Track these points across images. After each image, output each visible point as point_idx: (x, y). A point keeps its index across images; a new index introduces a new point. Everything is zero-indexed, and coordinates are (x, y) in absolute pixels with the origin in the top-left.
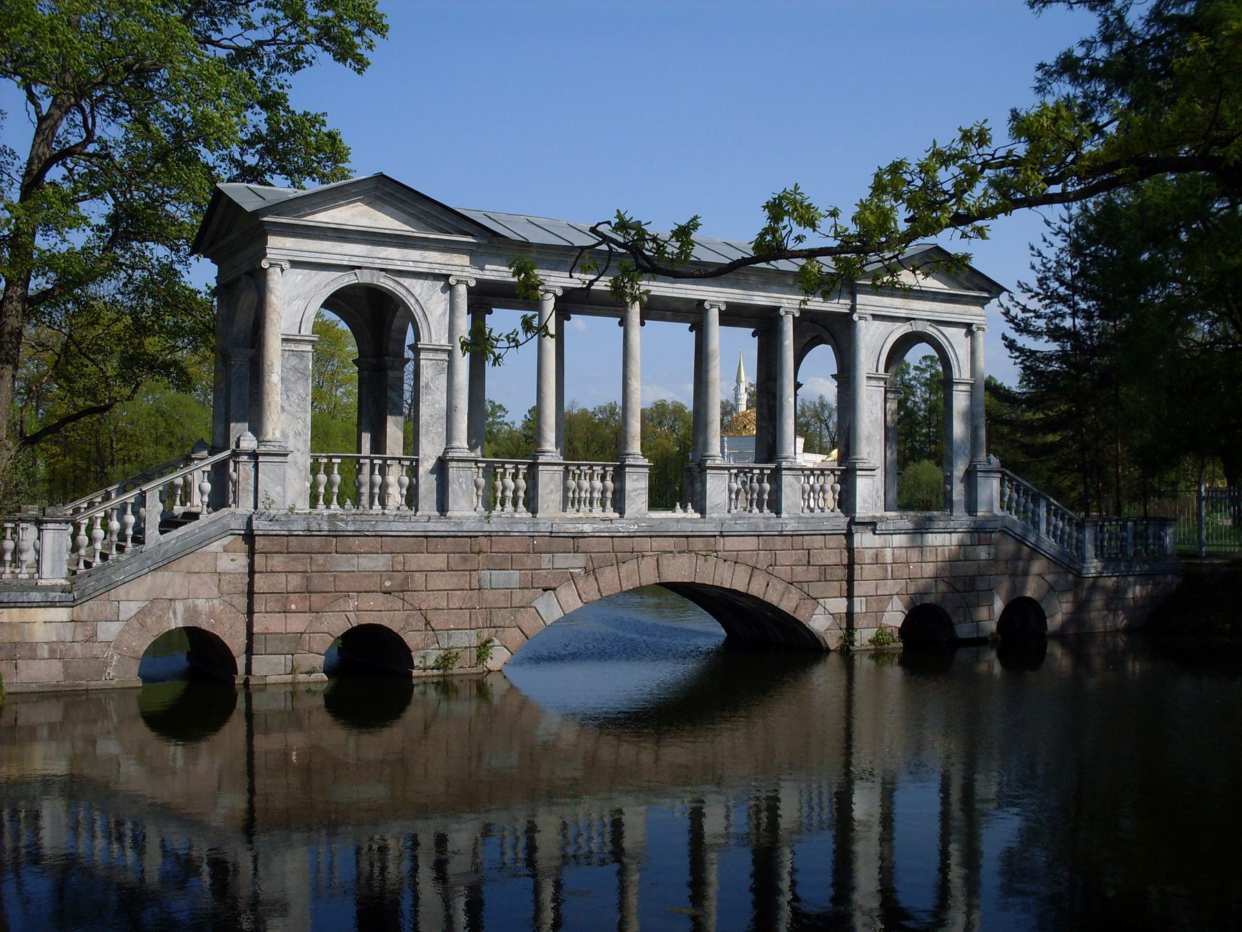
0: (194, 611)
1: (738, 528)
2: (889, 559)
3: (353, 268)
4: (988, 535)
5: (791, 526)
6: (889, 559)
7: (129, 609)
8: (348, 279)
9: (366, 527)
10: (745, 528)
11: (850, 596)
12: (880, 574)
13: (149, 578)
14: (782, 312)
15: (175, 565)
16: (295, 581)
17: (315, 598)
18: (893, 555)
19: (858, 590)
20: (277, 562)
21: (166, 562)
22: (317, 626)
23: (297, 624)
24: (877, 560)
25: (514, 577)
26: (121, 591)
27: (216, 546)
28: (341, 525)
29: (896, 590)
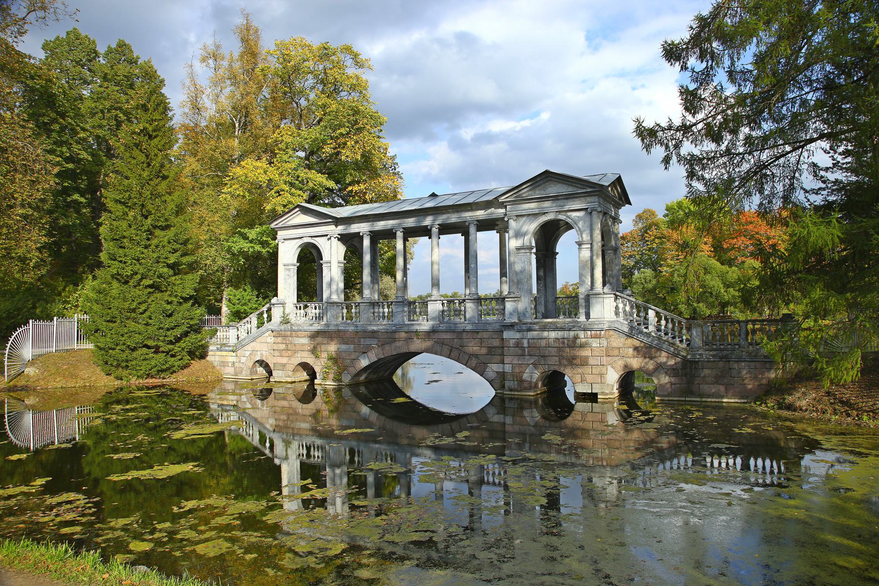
0: (262, 355)
1: (441, 328)
2: (526, 345)
3: (301, 238)
4: (598, 332)
5: (469, 327)
6: (526, 345)
7: (248, 353)
8: (300, 242)
9: (300, 328)
10: (444, 328)
11: (503, 363)
12: (520, 352)
13: (252, 344)
14: (467, 224)
15: (257, 340)
16: (283, 346)
17: (289, 352)
18: (528, 343)
19: (507, 360)
20: (279, 340)
21: (254, 340)
22: (290, 362)
23: (284, 360)
24: (518, 344)
25: (352, 346)
26: (245, 348)
27: (267, 334)
28: (294, 328)
29: (531, 362)
